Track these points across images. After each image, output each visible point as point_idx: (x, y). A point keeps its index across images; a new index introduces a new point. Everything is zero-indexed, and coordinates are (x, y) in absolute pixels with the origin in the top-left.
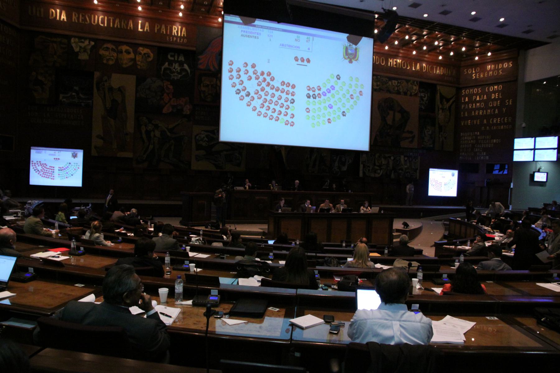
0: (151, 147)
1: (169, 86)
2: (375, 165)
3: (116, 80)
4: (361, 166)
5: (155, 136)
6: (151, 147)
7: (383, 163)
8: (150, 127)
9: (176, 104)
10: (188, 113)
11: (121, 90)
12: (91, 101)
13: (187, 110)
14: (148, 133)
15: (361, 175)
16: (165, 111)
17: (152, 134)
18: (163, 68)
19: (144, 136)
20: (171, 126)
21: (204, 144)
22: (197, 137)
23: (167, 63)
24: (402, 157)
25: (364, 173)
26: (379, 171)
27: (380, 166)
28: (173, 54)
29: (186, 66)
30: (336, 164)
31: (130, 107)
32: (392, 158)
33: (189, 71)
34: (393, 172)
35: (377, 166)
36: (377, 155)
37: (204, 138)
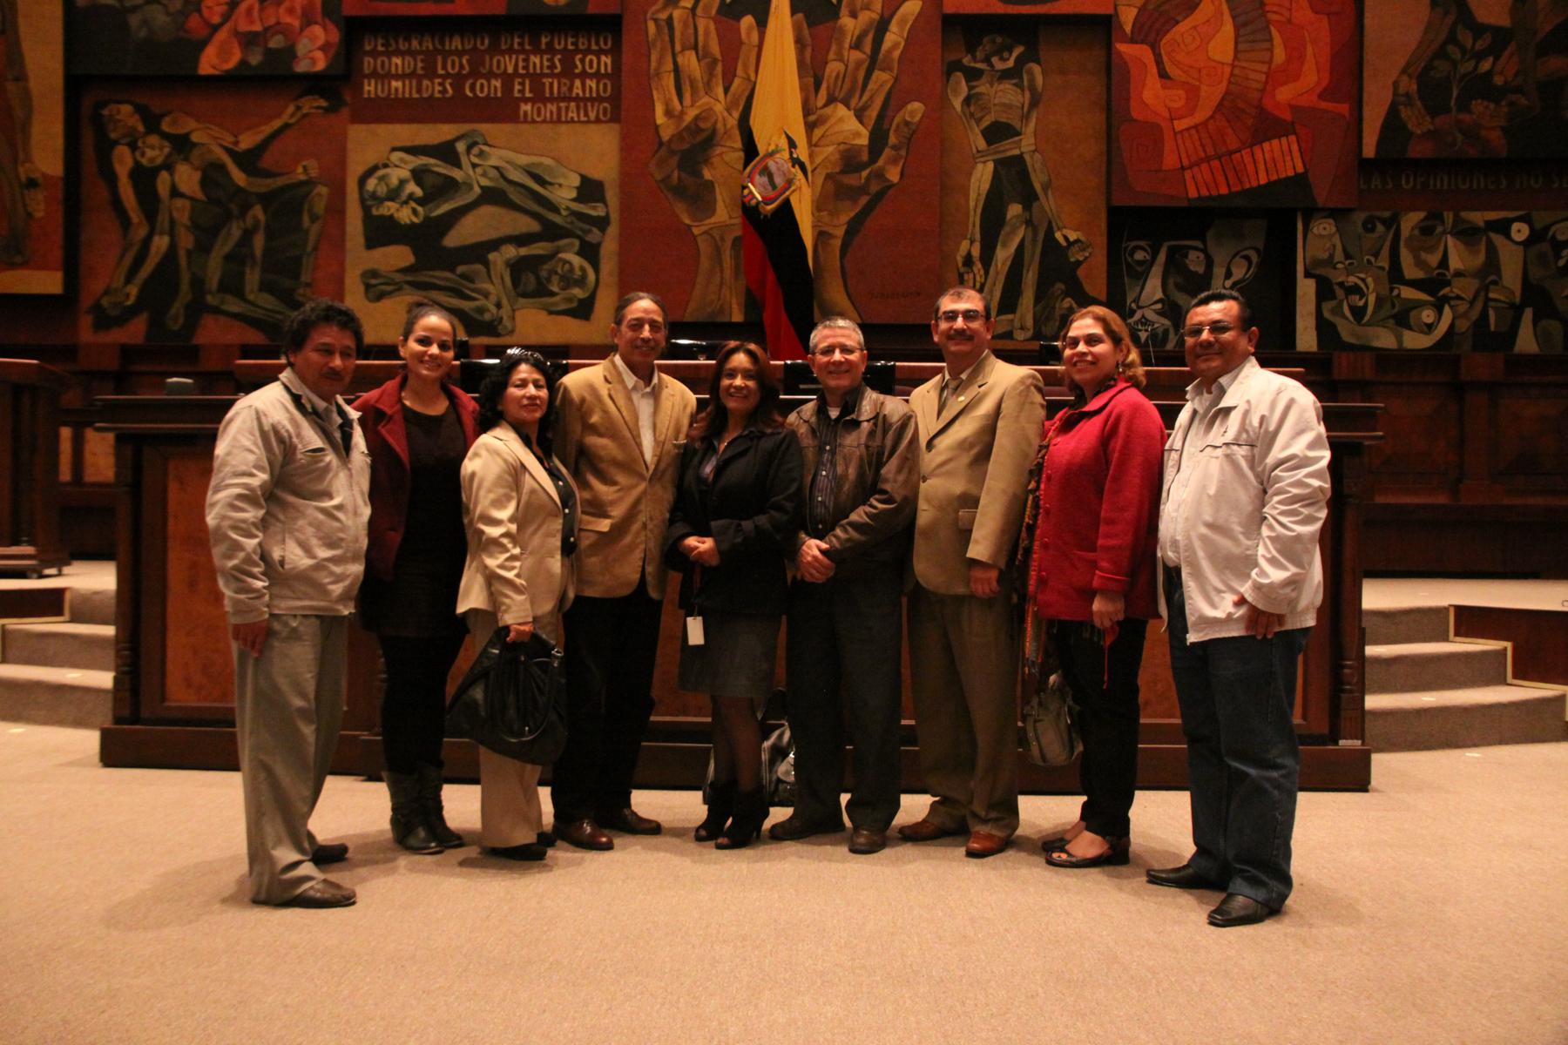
0: (161, 243)
2: (1396, 275)
4: (1306, 289)
5: (175, 192)
6: (161, 243)
7: (1455, 263)
8: (154, 151)
9: (257, 27)
10: (321, 65)
13: (314, 50)
14: (144, 178)
16: (210, 62)
17: (163, 182)
20: (247, 142)
21: (405, 215)
22: (371, 184)
25: (1325, 329)
26: (1428, 316)
27: (1434, 285)
30: (1153, 288)
34: (1528, 314)
35: (1415, 284)
36: (1411, 221)
37: (402, 182)
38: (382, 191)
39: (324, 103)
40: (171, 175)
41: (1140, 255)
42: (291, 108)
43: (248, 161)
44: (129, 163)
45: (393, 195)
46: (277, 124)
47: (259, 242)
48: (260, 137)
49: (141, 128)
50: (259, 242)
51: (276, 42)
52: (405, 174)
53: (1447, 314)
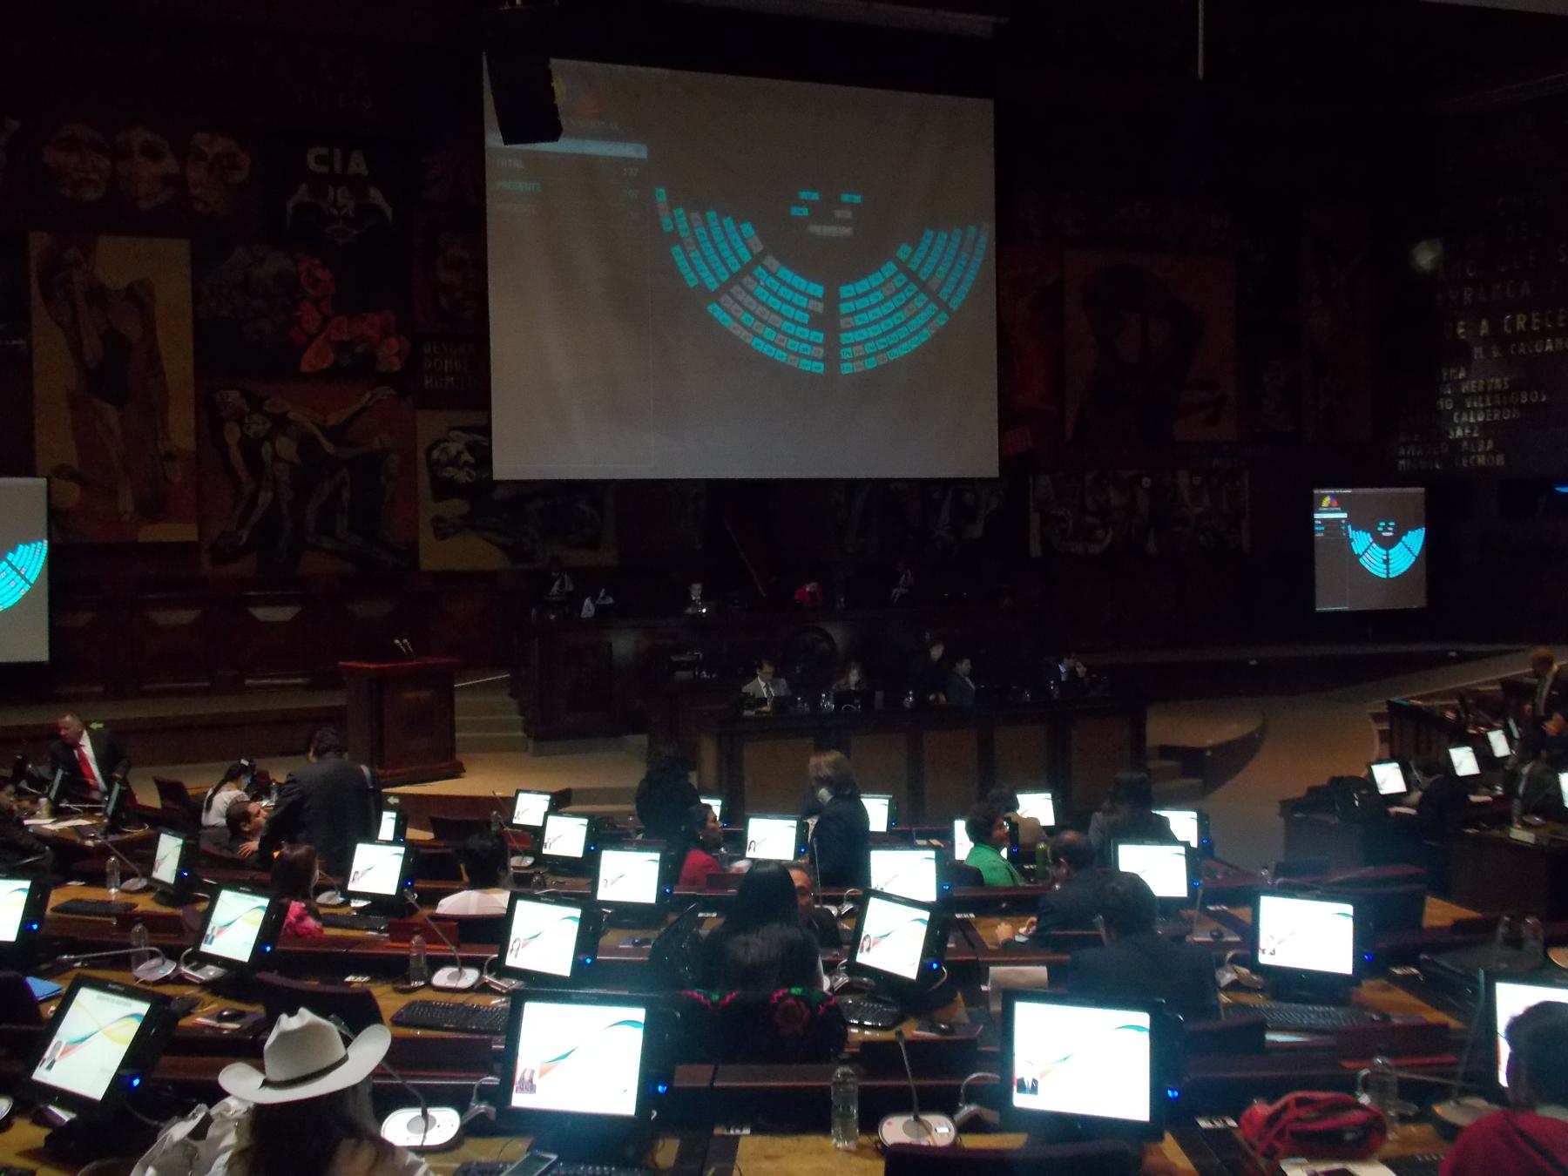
0: (265, 497)
1: (319, 273)
3: (118, 261)
4: (1035, 518)
5: (276, 457)
6: (265, 497)
8: (258, 426)
9: (346, 338)
10: (397, 368)
11: (139, 297)
12: (22, 342)
13: (390, 354)
14: (250, 448)
15: (1035, 549)
17: (266, 449)
18: (291, 204)
19: (236, 456)
20: (334, 419)
21: (462, 477)
22: (435, 454)
23: (303, 188)
24: (1183, 478)
26: (1100, 533)
28: (323, 151)
29: (376, 196)
31: (178, 362)
32: (1146, 482)
33: (389, 211)
37: (459, 453)
38: (444, 458)
39: (393, 392)
40: (273, 444)
41: (936, 495)
42: (368, 395)
43: (335, 434)
44: (238, 435)
45: (454, 462)
46: (357, 407)
47: (346, 495)
48: (344, 417)
49: (247, 409)
50: (346, 495)
51: (359, 350)
52: (460, 446)
53: (1111, 533)
